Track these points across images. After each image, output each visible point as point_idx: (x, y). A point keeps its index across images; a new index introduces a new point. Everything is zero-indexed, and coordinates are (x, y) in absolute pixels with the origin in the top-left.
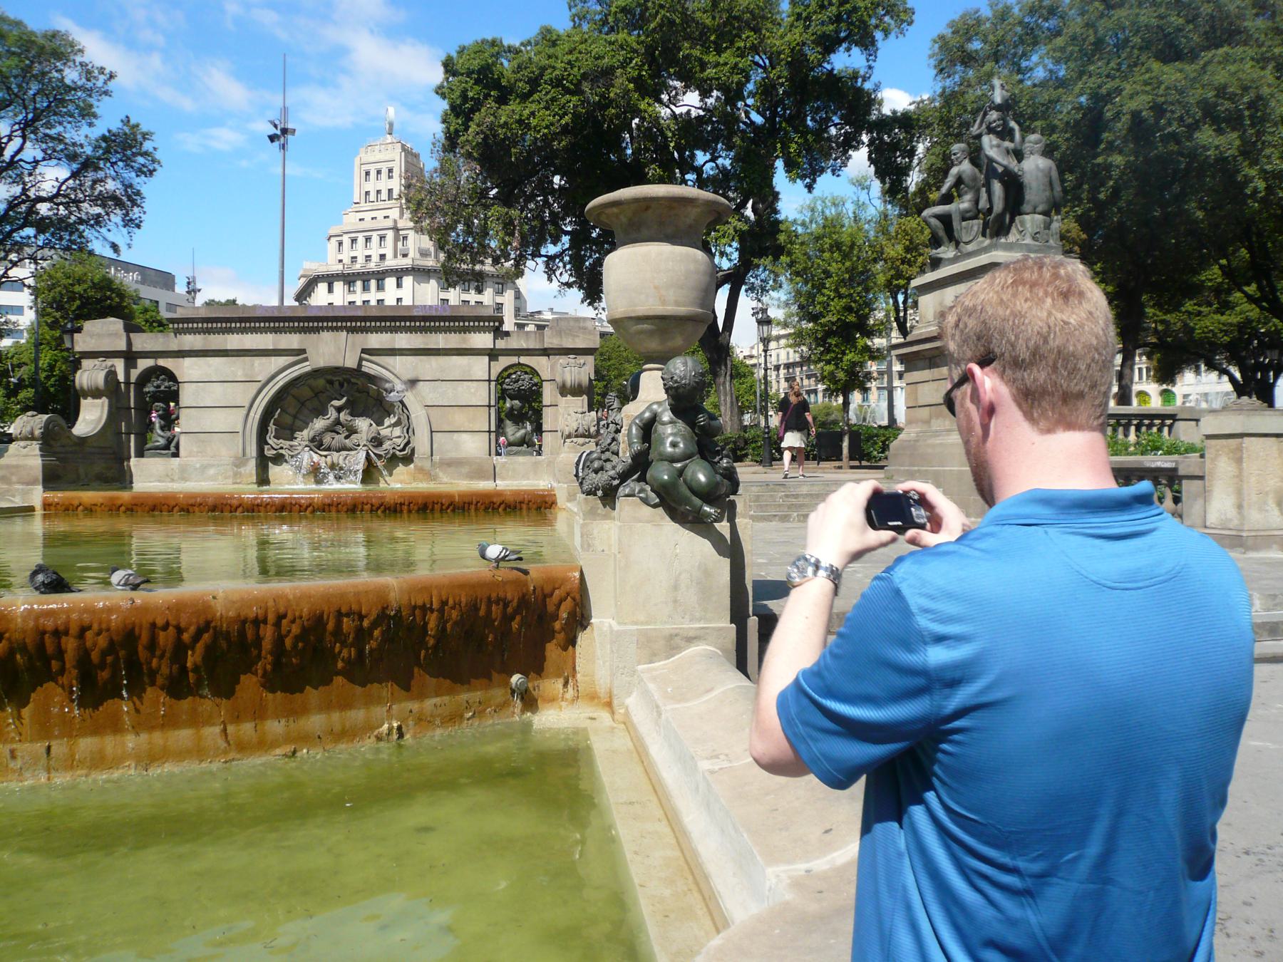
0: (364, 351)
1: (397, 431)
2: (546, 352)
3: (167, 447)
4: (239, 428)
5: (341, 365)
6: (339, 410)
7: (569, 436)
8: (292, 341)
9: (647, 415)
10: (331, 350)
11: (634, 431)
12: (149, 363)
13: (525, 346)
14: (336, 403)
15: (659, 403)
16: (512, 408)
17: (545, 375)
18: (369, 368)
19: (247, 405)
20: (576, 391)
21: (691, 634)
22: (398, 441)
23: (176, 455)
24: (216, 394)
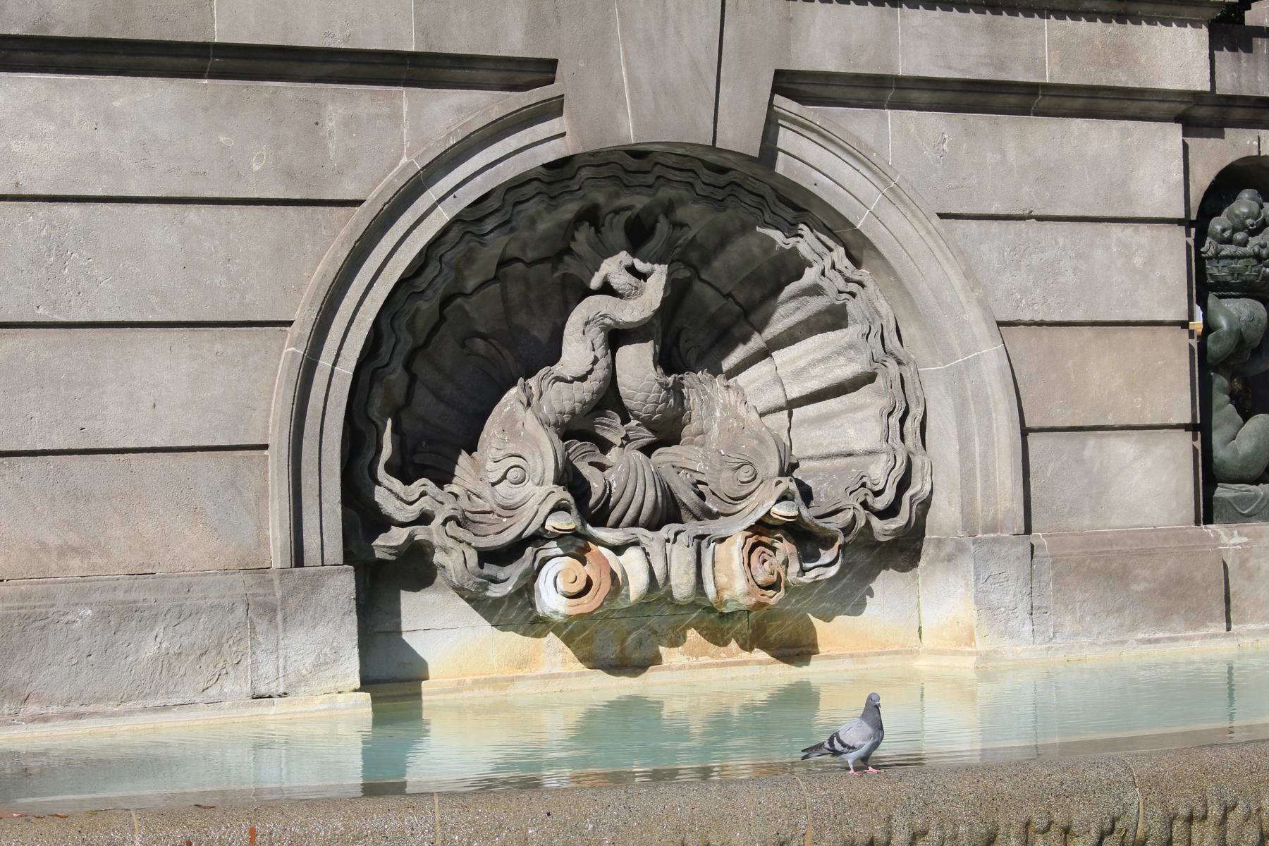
0: (788, 83)
1: (857, 427)
6: (616, 337)
18: (807, 159)
19: (304, 316)
24: (155, 260)
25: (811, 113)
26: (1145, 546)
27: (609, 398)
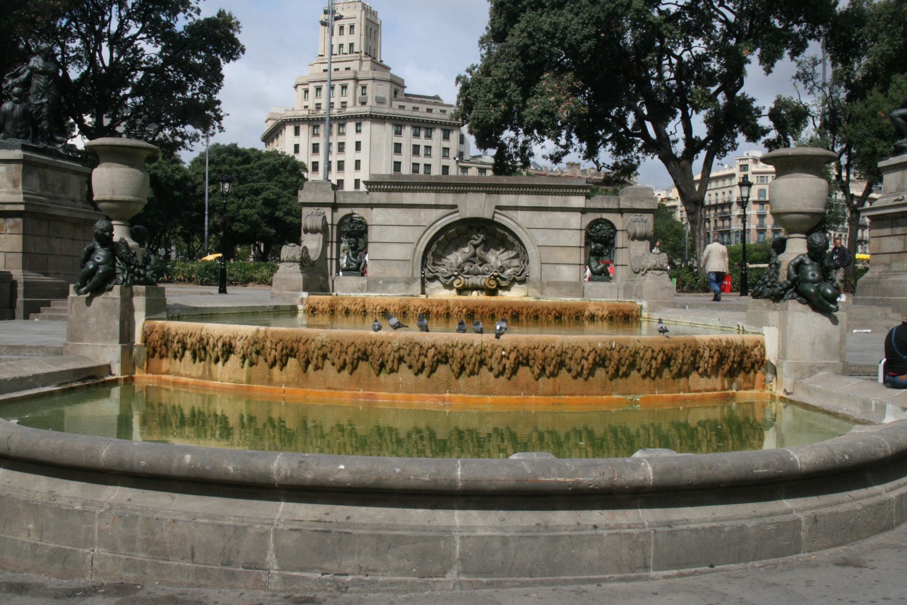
0: (498, 207)
1: (516, 262)
2: (621, 211)
3: (357, 269)
4: (409, 257)
5: (481, 216)
6: (476, 247)
7: (649, 269)
8: (448, 199)
9: (797, 261)
10: (475, 206)
11: (791, 268)
12: (348, 211)
13: (606, 206)
14: (472, 241)
15: (803, 255)
16: (596, 249)
17: (618, 226)
18: (499, 218)
20: (642, 238)
21: (821, 365)
22: (517, 269)
23: (363, 275)
24: (394, 234)
25: (502, 212)
26: (567, 284)
27: (474, 255)
